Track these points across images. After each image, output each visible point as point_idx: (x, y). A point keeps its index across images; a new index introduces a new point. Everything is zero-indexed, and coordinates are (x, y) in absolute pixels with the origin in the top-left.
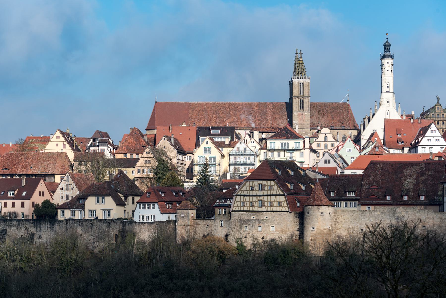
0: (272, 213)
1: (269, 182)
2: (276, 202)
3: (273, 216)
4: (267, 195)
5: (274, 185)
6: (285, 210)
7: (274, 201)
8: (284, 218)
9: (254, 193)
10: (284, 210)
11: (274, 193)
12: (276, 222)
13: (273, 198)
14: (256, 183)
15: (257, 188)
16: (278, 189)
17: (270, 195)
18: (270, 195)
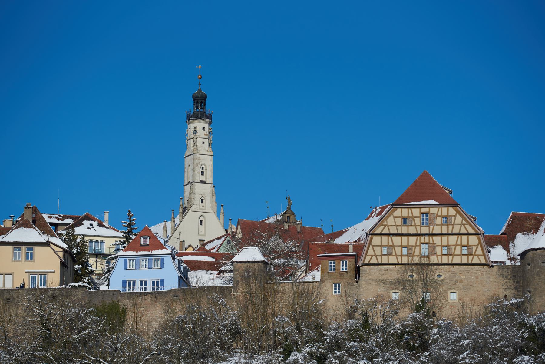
0: (451, 267)
1: (445, 210)
2: (458, 248)
3: (454, 273)
4: (441, 234)
5: (455, 216)
6: (479, 262)
7: (456, 245)
8: (477, 278)
9: (412, 230)
10: (476, 261)
11: (456, 231)
12: (461, 285)
13: (453, 240)
14: (416, 212)
15: (418, 221)
16: (464, 222)
17: (448, 234)
18: (448, 234)
